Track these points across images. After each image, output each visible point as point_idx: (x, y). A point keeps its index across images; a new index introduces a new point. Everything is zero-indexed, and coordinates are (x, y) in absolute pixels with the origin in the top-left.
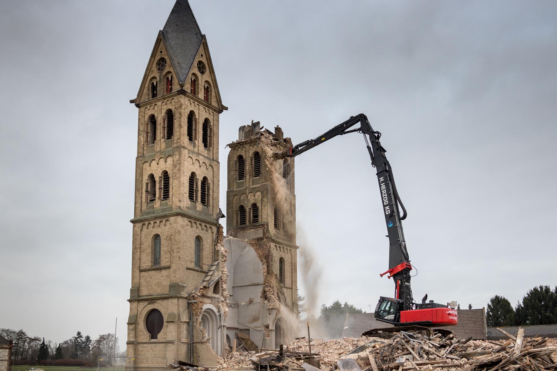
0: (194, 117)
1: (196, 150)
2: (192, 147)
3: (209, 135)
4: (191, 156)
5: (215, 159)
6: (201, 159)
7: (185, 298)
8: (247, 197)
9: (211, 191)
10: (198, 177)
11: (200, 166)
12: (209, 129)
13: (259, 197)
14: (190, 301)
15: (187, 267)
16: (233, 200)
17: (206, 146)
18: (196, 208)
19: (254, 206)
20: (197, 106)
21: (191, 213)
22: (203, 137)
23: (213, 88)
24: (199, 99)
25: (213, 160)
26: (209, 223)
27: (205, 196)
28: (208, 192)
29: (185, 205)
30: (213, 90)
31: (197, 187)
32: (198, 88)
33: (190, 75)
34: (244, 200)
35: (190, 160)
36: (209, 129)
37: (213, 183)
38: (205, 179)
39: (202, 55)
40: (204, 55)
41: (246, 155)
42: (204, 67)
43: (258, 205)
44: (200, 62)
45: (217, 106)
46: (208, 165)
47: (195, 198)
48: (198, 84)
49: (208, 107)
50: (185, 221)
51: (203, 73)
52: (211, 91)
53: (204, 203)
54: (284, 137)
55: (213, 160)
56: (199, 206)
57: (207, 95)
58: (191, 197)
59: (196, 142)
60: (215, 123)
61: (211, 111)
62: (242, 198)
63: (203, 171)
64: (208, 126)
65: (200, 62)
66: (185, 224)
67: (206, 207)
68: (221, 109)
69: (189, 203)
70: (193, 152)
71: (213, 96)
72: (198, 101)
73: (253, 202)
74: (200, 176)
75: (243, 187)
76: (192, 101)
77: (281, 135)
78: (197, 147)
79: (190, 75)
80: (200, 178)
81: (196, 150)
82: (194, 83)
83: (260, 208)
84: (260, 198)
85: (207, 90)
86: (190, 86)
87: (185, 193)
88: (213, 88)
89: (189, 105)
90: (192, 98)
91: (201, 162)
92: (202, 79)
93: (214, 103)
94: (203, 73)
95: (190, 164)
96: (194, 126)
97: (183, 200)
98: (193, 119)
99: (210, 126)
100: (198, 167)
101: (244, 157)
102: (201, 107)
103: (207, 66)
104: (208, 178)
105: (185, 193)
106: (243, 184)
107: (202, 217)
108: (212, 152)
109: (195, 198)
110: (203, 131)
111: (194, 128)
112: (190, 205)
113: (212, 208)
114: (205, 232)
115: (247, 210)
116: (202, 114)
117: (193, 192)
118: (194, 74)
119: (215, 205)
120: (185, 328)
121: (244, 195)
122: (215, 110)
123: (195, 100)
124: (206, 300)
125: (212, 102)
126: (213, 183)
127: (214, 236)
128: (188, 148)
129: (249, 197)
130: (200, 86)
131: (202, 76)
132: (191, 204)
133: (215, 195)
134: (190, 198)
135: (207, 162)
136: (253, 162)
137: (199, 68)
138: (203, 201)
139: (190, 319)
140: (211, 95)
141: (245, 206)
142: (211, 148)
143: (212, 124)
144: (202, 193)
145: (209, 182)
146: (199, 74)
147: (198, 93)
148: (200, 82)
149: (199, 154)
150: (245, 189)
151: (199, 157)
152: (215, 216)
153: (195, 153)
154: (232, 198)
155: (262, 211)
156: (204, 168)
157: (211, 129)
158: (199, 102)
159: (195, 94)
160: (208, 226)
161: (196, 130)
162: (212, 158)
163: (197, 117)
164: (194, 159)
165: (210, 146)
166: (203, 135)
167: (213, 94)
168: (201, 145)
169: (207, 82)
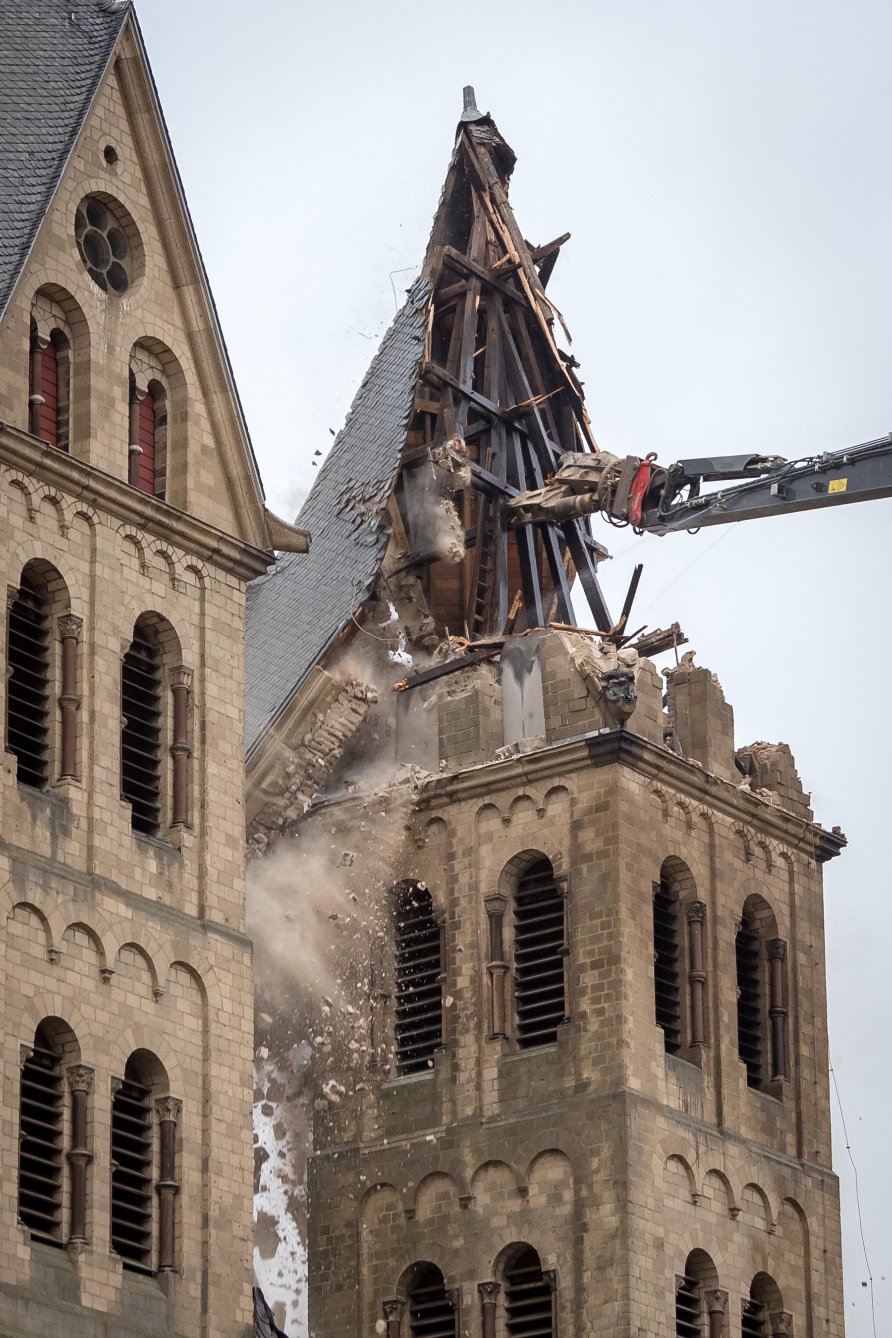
0: (57, 611)
1: (73, 851)
2: (43, 833)
3: (167, 737)
4: (35, 897)
5: (215, 916)
6: (113, 917)
8: (465, 1202)
10: (87, 1058)
11: (105, 974)
12: (168, 698)
13: (556, 1199)
16: (354, 1225)
17: (144, 822)
18: (71, 1289)
19: (522, 1263)
20: (78, 530)
22: (126, 754)
23: (193, 391)
24: (89, 472)
25: (204, 925)
27: (143, 1200)
28: (168, 1168)
30: (198, 408)
31: (78, 1137)
32: (85, 393)
33: (23, 300)
34: (441, 1222)
35: (25, 928)
36: (168, 698)
37: (206, 1100)
38: (142, 1068)
39: (110, 154)
40: (126, 152)
41: (453, 879)
42: (125, 238)
43: (550, 1261)
44: (97, 207)
45: (225, 523)
46: (162, 964)
47: (64, 1215)
48: (85, 367)
49: (164, 533)
51: (116, 282)
52: (184, 417)
53: (140, 1254)
54: (742, 739)
55: (204, 925)
56: (101, 1278)
57: (155, 448)
58: (37, 1208)
59: (76, 795)
60: (212, 651)
61: (182, 559)
62: (425, 1211)
63: (126, 1012)
64: (162, 674)
65: (97, 207)
68: (255, 541)
69: (24, 1252)
70: (51, 871)
71: (193, 448)
72: (82, 492)
73: (511, 1236)
74: (103, 1046)
75: (432, 1121)
76: (38, 490)
77: (714, 724)
78: (78, 832)
79: (23, 300)
80: (106, 1067)
81: (73, 851)
82: (54, 357)
83: (565, 1283)
84: (566, 1209)
85: (151, 408)
86: (23, 383)
88: (193, 391)
89: (18, 520)
90: (39, 471)
91: (111, 944)
92: (117, 329)
93: (207, 504)
94: (116, 282)
95: (28, 962)
96: (55, 674)
98: (52, 624)
99: (179, 670)
100: (91, 984)
101: (440, 899)
102: (110, 535)
103: (148, 233)
104: (169, 1063)
106: (436, 1099)
108: (191, 867)
109: (64, 1215)
110: (127, 707)
111: (55, 689)
112: (26, 1274)
113: (194, 1290)
115: (470, 1299)
116: (112, 585)
117: (54, 1172)
118: (52, 294)
119: (218, 1267)
121: (440, 1186)
122: (213, 556)
123: (63, 483)
125: (193, 497)
126: (206, 1100)
128: (14, 839)
129: (482, 1199)
130: (97, 382)
131: (112, 307)
132: (36, 1260)
134: (26, 1219)
135: (159, 940)
136: (509, 934)
137: (92, 251)
138: (129, 1241)
140: (182, 444)
141: (452, 1272)
142: (188, 840)
143: (190, 658)
144: (117, 1176)
145: (176, 1090)
146: (88, 293)
147: (85, 433)
148: (97, 353)
149: (93, 884)
150: (449, 1142)
151: (93, 906)
153: (66, 874)
154: (347, 1208)
155: (578, 1304)
156: (132, 989)
157: (181, 696)
158: (93, 492)
159: (60, 439)
161: (69, 704)
162: (191, 910)
163: (79, 609)
164: (57, 924)
165: (179, 819)
166: (126, 737)
167: (200, 435)
168: (114, 814)
169: (148, 346)
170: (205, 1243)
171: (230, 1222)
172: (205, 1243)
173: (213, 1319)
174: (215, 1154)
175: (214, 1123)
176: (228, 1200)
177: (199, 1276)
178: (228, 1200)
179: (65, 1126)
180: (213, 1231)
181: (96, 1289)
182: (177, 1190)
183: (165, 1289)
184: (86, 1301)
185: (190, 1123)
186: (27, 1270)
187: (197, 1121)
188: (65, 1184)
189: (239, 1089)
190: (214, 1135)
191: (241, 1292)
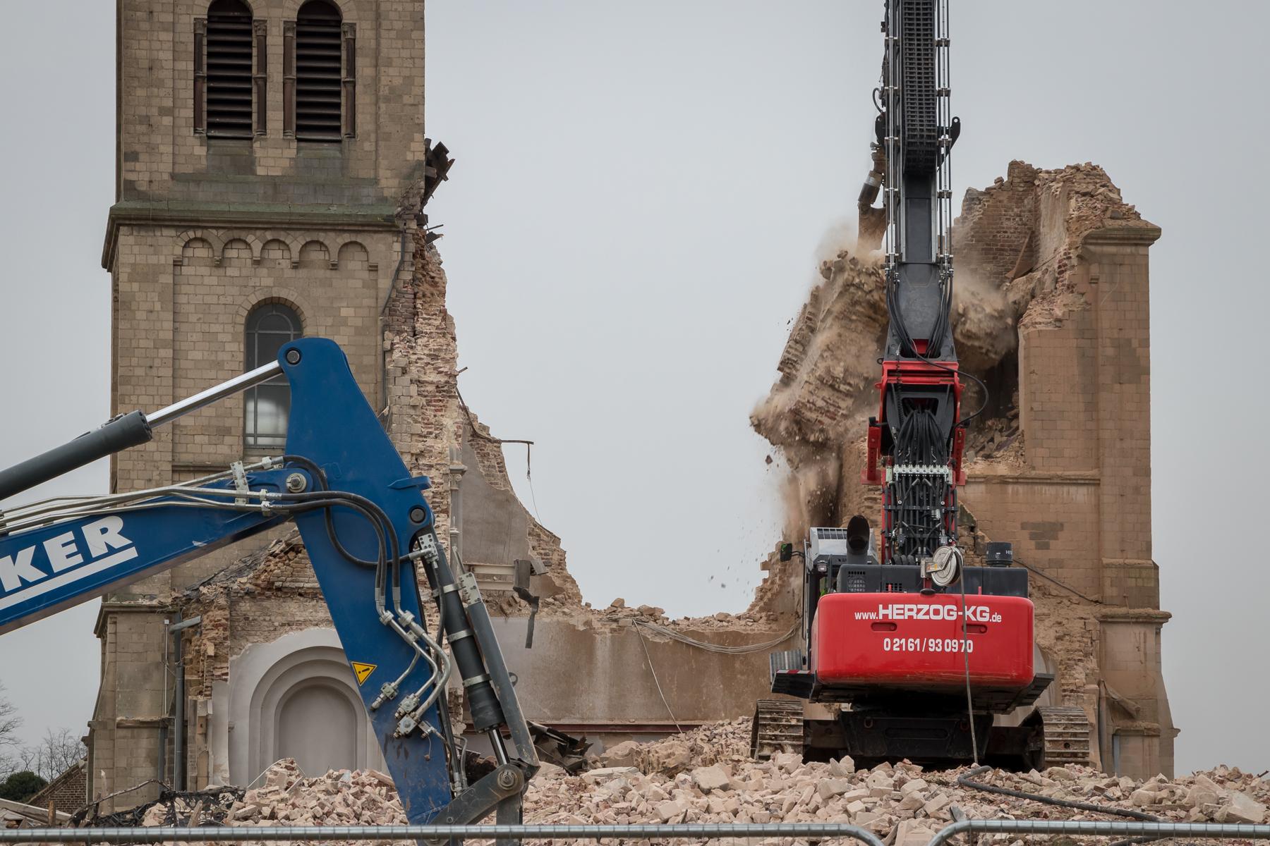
7: (151, 610)
9: (364, 68)
14: (178, 626)
15: (186, 458)
18: (248, 165)
21: (207, 199)
26: (336, 227)
28: (352, 71)
29: (165, 167)
31: (263, 66)
37: (378, 16)
50: (168, 244)
56: (275, 153)
66: (165, 259)
67: (329, 150)
69: (201, 151)
87: (163, 111)
97: (152, 149)
105: (163, 111)
107: (303, 204)
113: (368, 146)
114: (322, 273)
120: (142, 753)
124: (294, 608)
126: (378, 16)
127: (385, 283)
133: (392, 76)
139: (172, 711)
152: (390, 184)
160: (334, 241)
170: (377, 116)
171: (401, 96)
172: (377, 116)
173: (383, 163)
174: (384, 52)
175: (383, 33)
176: (398, 81)
177: (373, 137)
178: (398, 81)
179: (254, 61)
180: (383, 106)
181: (271, 162)
182: (354, 84)
183: (341, 151)
184: (260, 171)
185: (364, 35)
186: (204, 162)
187: (370, 34)
188: (254, 98)
189: (409, 7)
190: (383, 41)
191: (412, 140)
